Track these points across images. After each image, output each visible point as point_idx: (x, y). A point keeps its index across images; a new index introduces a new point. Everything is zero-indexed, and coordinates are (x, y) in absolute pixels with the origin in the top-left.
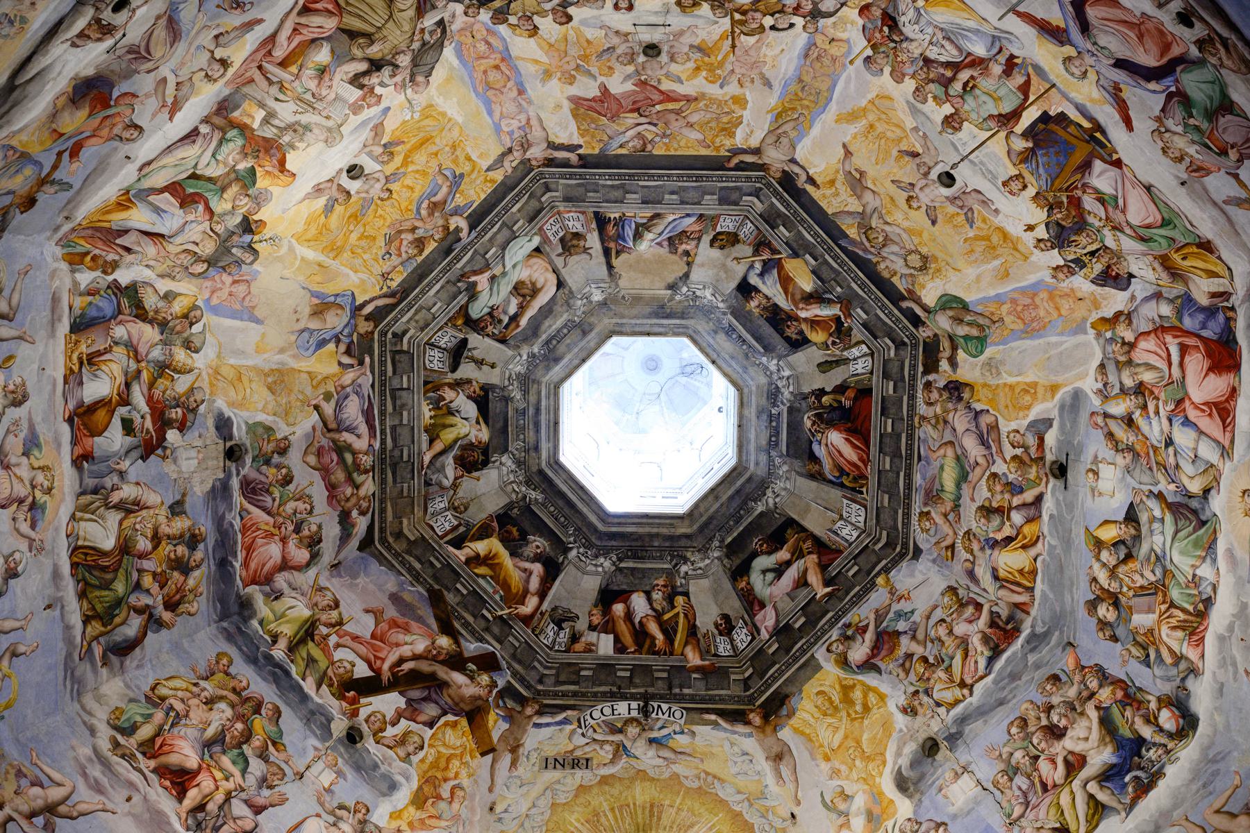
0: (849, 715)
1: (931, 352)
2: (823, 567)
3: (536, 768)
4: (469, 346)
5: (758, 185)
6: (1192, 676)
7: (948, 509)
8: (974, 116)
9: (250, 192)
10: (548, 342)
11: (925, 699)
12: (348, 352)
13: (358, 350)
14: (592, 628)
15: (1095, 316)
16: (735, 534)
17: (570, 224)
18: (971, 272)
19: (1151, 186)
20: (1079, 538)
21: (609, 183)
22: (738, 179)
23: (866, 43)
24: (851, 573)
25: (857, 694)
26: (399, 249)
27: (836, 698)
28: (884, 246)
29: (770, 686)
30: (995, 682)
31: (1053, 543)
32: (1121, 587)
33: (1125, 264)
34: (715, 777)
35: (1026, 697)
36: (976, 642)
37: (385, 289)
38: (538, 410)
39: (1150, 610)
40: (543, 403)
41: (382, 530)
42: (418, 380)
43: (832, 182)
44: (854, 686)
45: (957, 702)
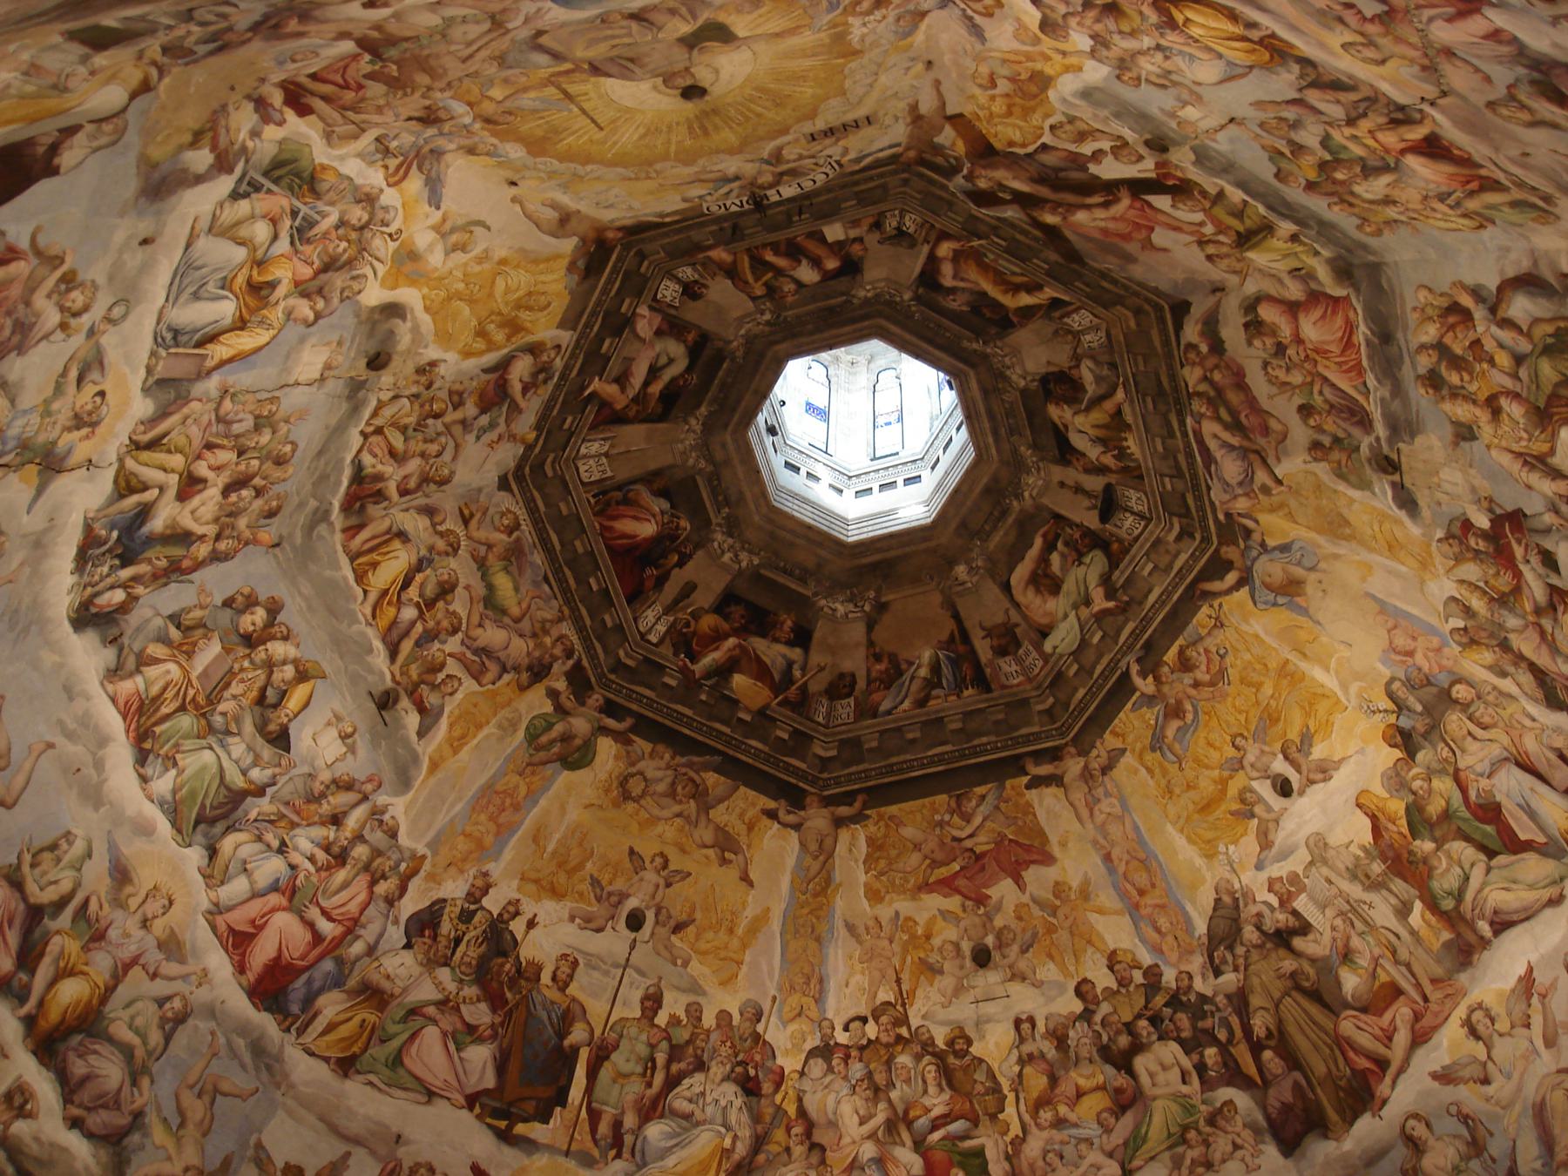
0: (500, 314)
1: (579, 682)
2: (604, 403)
3: (881, 113)
4: (1096, 512)
5: (825, 775)
6: (113, 666)
7: (490, 556)
8: (633, 1031)
9: (1411, 798)
10: (1004, 513)
11: (414, 390)
12: (1248, 533)
13: (1234, 530)
14: (860, 240)
15: (427, 866)
16: (721, 373)
17: (1014, 667)
18: (574, 814)
19: (429, 1102)
20: (328, 662)
21: (984, 740)
22: (850, 779)
23: (767, 1038)
24: (569, 420)
25: (499, 336)
26: (1209, 661)
27: (525, 316)
28: (673, 784)
29: (611, 273)
30: (342, 460)
31: (355, 627)
32: (252, 662)
33: (420, 957)
34: (637, 179)
35: (293, 482)
36: (388, 469)
37: (1216, 604)
38: (995, 433)
39: (205, 674)
40: (990, 440)
41: (1162, 320)
42: (1151, 481)
43: (751, 828)
44: (509, 338)
45: (375, 414)
